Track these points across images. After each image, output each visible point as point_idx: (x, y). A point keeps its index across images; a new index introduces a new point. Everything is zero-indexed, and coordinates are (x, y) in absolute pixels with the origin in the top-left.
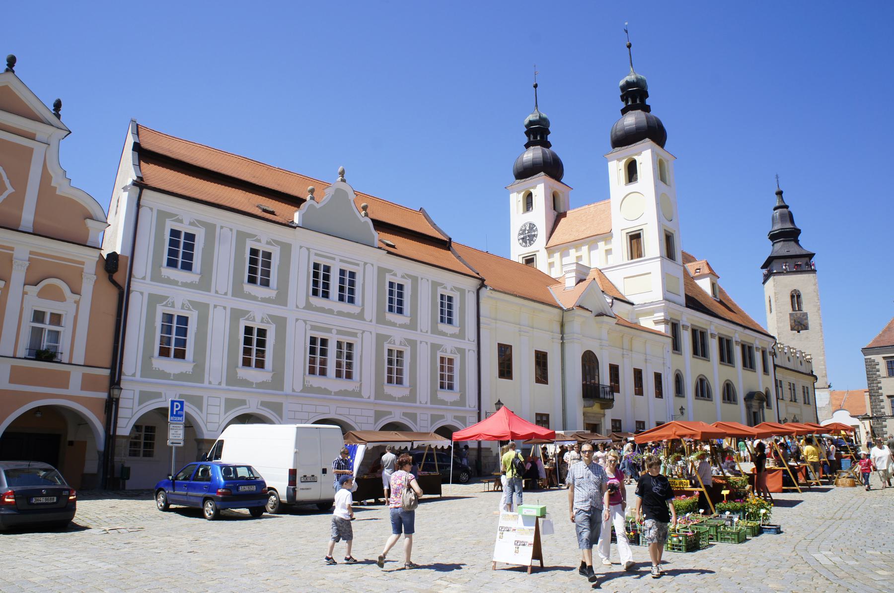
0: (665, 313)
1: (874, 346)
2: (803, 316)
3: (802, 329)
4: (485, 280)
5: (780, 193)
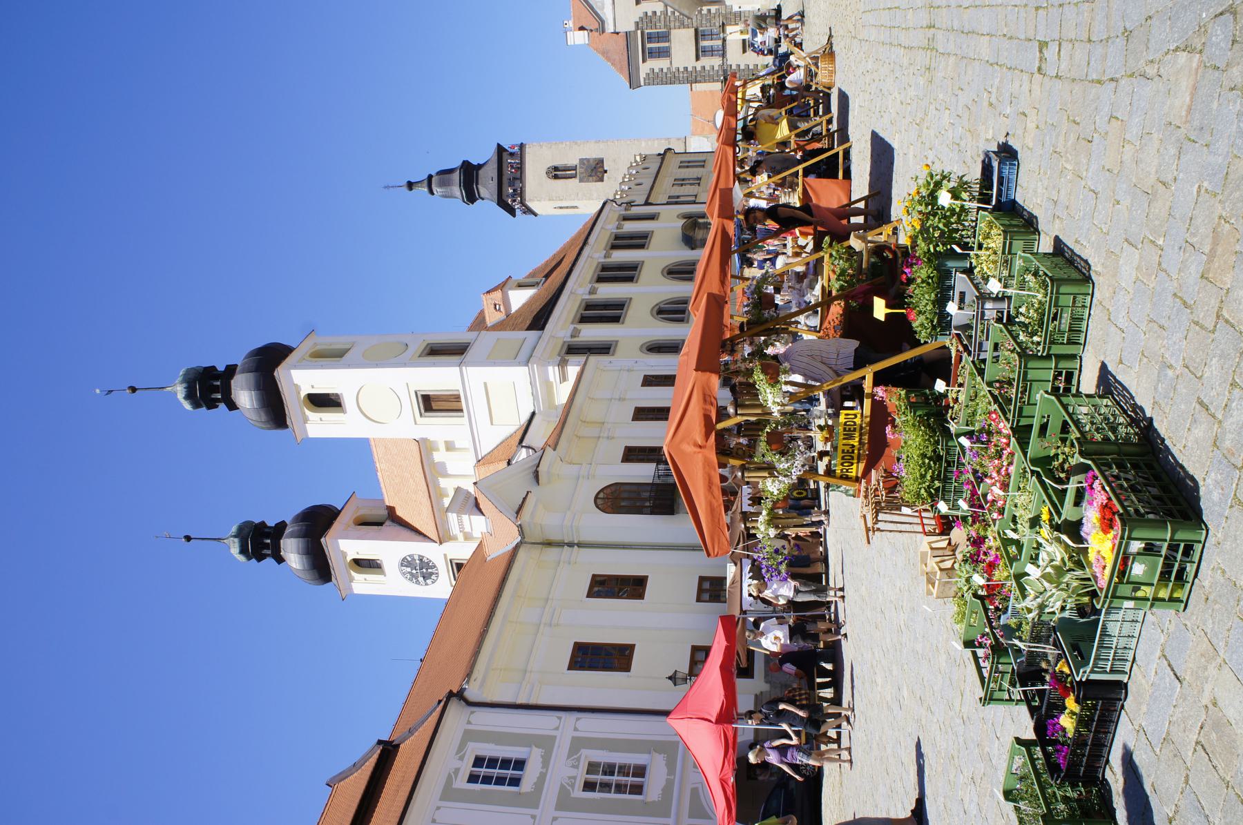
0: (549, 364)
1: (628, 72)
2: (584, 164)
3: (603, 167)
4: (451, 691)
5: (410, 185)
